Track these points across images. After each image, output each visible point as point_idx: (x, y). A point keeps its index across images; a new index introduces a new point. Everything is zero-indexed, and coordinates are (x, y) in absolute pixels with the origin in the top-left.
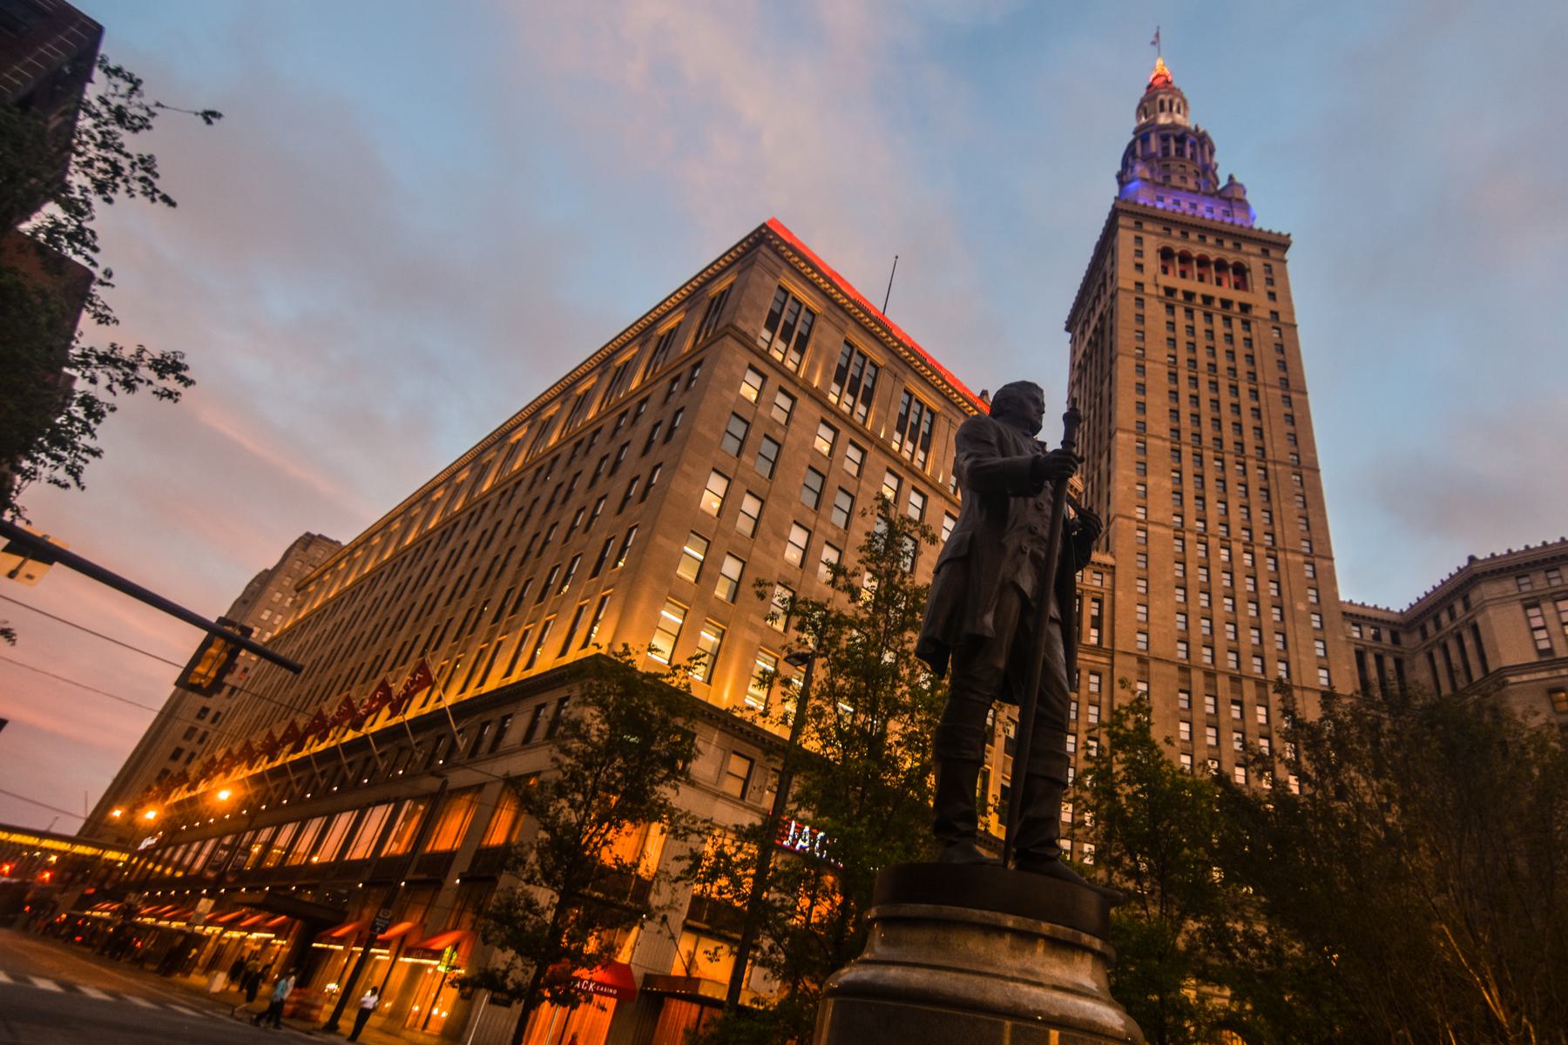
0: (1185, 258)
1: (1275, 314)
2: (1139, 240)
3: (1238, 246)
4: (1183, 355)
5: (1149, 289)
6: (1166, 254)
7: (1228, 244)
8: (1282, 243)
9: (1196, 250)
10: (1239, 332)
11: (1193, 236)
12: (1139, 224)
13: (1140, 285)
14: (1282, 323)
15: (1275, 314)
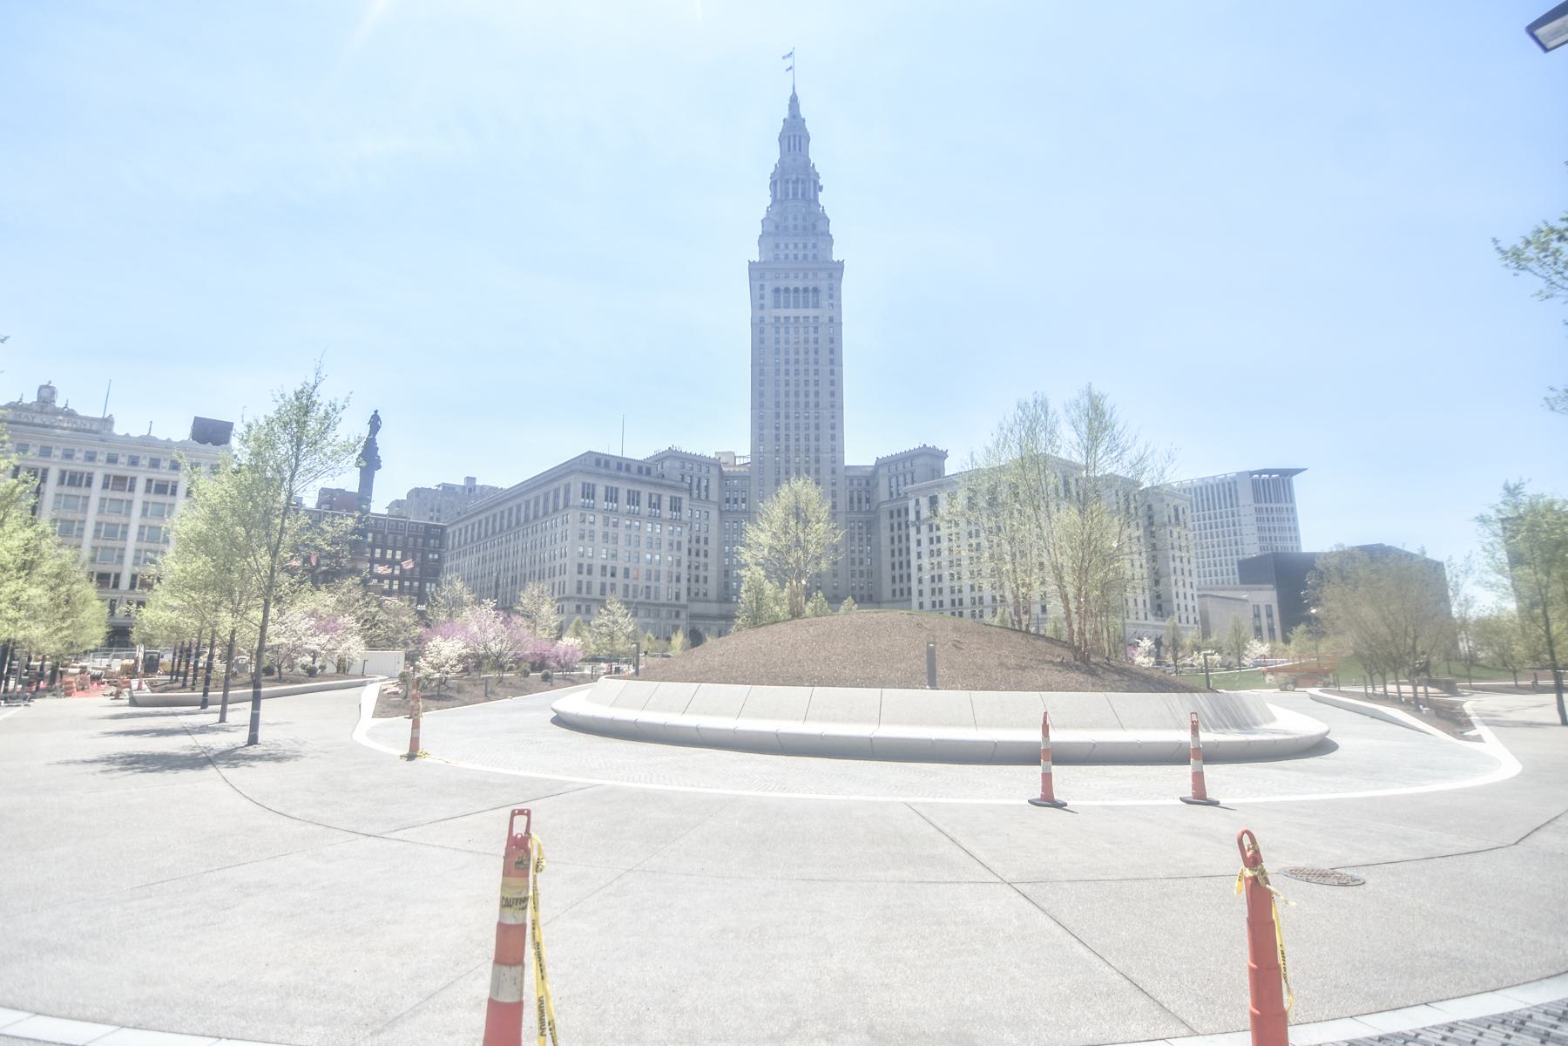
0: (787, 290)
1: (831, 320)
2: (762, 287)
3: (815, 275)
4: (782, 357)
5: (767, 320)
6: (777, 290)
7: (810, 275)
8: (840, 266)
9: (792, 284)
10: (812, 336)
11: (792, 275)
12: (762, 277)
13: (762, 320)
14: (835, 323)
15: (831, 320)
